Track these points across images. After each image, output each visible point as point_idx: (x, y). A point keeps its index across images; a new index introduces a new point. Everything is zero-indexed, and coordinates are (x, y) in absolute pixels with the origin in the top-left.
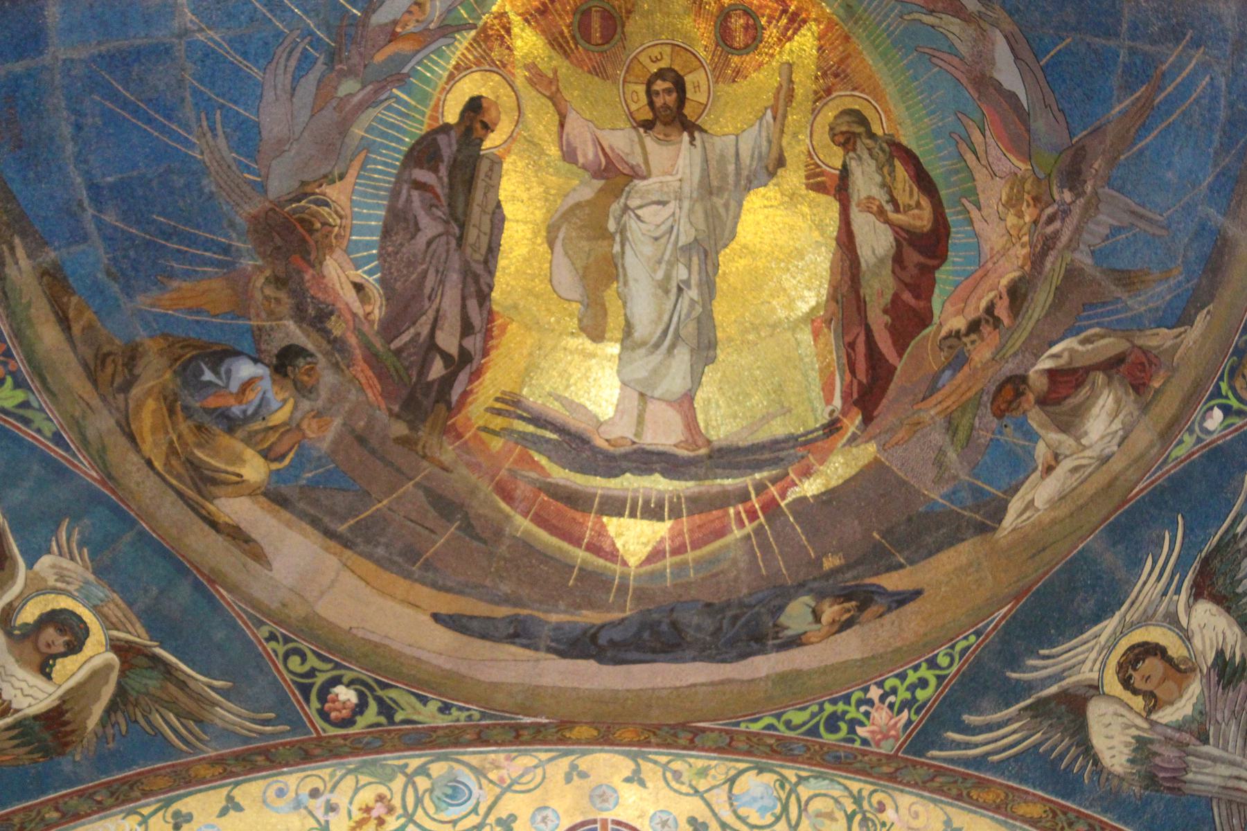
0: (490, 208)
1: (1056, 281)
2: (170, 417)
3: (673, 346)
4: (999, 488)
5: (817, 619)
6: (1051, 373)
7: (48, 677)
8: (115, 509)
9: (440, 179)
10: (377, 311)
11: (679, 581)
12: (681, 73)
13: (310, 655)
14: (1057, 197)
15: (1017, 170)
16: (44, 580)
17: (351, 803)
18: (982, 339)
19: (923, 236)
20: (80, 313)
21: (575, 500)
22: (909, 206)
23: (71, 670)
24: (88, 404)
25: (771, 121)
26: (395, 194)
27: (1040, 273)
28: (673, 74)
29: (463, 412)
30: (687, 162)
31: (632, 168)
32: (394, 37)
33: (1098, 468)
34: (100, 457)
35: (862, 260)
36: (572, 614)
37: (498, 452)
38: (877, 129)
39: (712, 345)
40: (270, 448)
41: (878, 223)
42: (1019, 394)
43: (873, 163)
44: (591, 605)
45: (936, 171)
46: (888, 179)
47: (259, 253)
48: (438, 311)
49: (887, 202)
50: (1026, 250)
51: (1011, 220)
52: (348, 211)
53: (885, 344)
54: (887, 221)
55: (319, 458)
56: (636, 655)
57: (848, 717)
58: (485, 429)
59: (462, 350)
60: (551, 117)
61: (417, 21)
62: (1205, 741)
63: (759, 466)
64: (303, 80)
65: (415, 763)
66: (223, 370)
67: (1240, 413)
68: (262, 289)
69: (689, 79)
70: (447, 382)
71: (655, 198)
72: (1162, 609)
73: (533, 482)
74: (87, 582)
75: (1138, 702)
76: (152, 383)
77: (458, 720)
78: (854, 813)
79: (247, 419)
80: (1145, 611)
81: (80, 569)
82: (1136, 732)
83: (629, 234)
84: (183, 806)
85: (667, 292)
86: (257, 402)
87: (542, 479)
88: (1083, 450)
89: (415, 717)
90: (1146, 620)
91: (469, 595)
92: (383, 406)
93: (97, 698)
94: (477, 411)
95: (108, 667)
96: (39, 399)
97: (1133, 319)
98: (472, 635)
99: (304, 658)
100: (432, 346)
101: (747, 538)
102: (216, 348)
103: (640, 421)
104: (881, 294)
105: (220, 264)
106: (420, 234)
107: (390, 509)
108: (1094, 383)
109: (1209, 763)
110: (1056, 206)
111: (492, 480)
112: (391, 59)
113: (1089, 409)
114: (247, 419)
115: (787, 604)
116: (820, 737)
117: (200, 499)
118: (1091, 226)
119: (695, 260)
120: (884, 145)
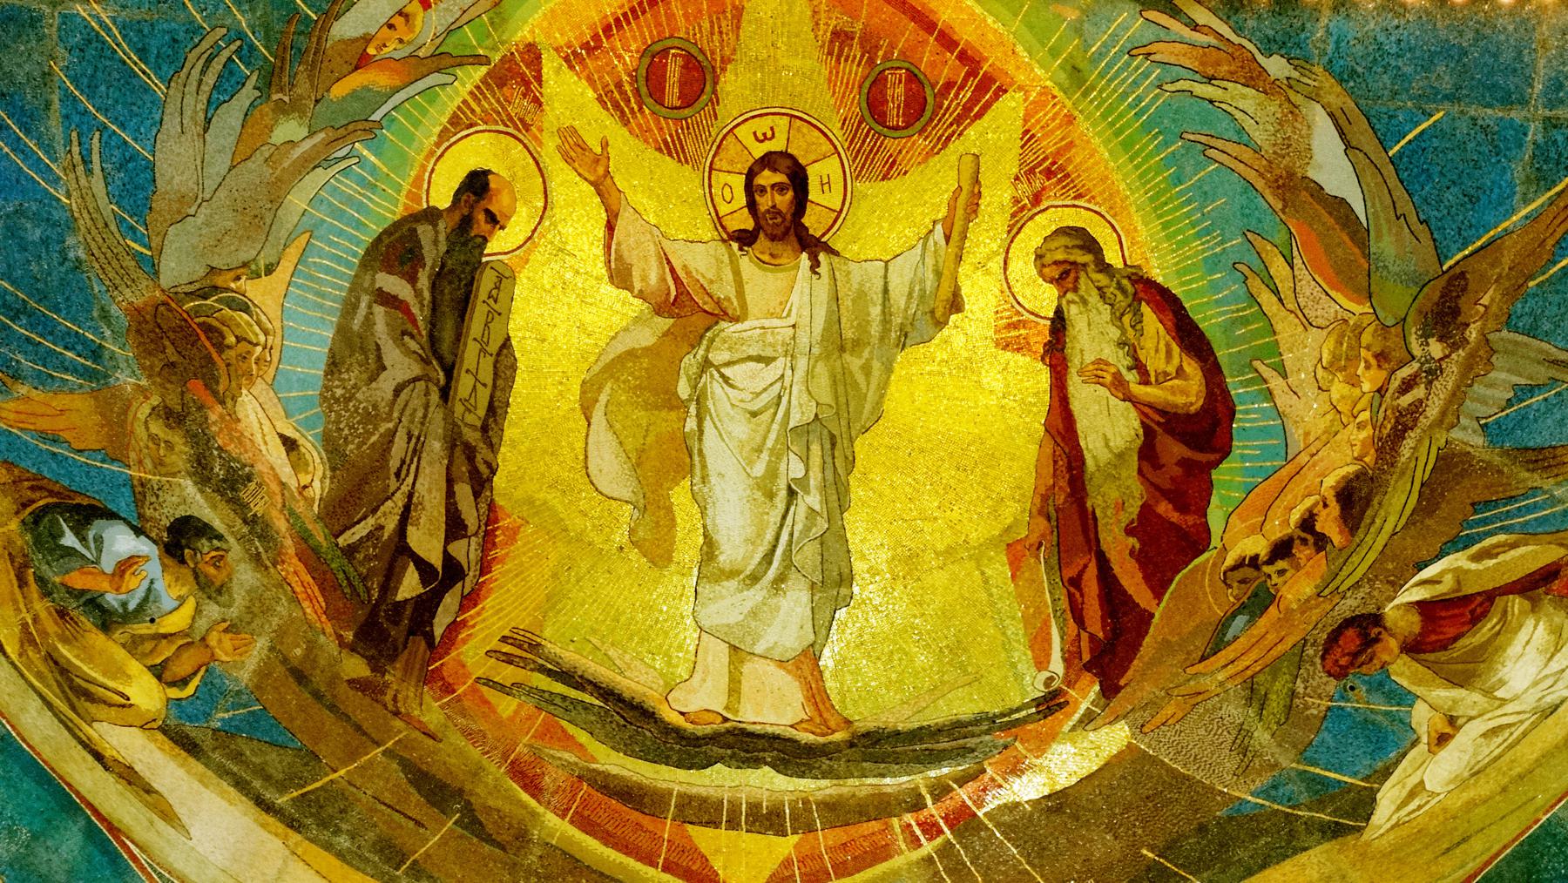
0: (493, 347)
3: (781, 579)
4: (1355, 775)
6: (1421, 605)
9: (418, 294)
10: (317, 484)
12: (803, 162)
14: (1417, 351)
15: (1347, 315)
18: (1298, 568)
22: (1166, 374)
25: (943, 242)
26: (350, 308)
28: (788, 162)
29: (454, 654)
30: (806, 298)
31: (718, 303)
32: (362, 62)
33: (1534, 726)
35: (1087, 456)
37: (512, 719)
38: (1112, 257)
39: (846, 579)
41: (1114, 401)
42: (1369, 642)
45: (1209, 320)
46: (1131, 332)
47: (143, 368)
48: (410, 495)
49: (1130, 369)
50: (1367, 433)
51: (1339, 389)
52: (277, 325)
54: (1128, 398)
55: (239, 693)
58: (488, 682)
59: (448, 558)
61: (401, 41)
63: (935, 758)
66: (91, 535)
69: (813, 173)
70: (426, 606)
71: (753, 352)
73: (567, 765)
79: (128, 617)
83: (710, 404)
85: (771, 496)
87: (582, 764)
88: (1500, 706)
92: (329, 630)
100: (401, 550)
102: (78, 500)
103: (734, 689)
104: (1121, 506)
105: (89, 374)
106: (384, 375)
108: (1505, 612)
110: (1416, 365)
111: (505, 756)
112: (354, 94)
113: (1501, 649)
114: (128, 617)
118: (1478, 388)
119: (815, 448)
120: (1125, 282)
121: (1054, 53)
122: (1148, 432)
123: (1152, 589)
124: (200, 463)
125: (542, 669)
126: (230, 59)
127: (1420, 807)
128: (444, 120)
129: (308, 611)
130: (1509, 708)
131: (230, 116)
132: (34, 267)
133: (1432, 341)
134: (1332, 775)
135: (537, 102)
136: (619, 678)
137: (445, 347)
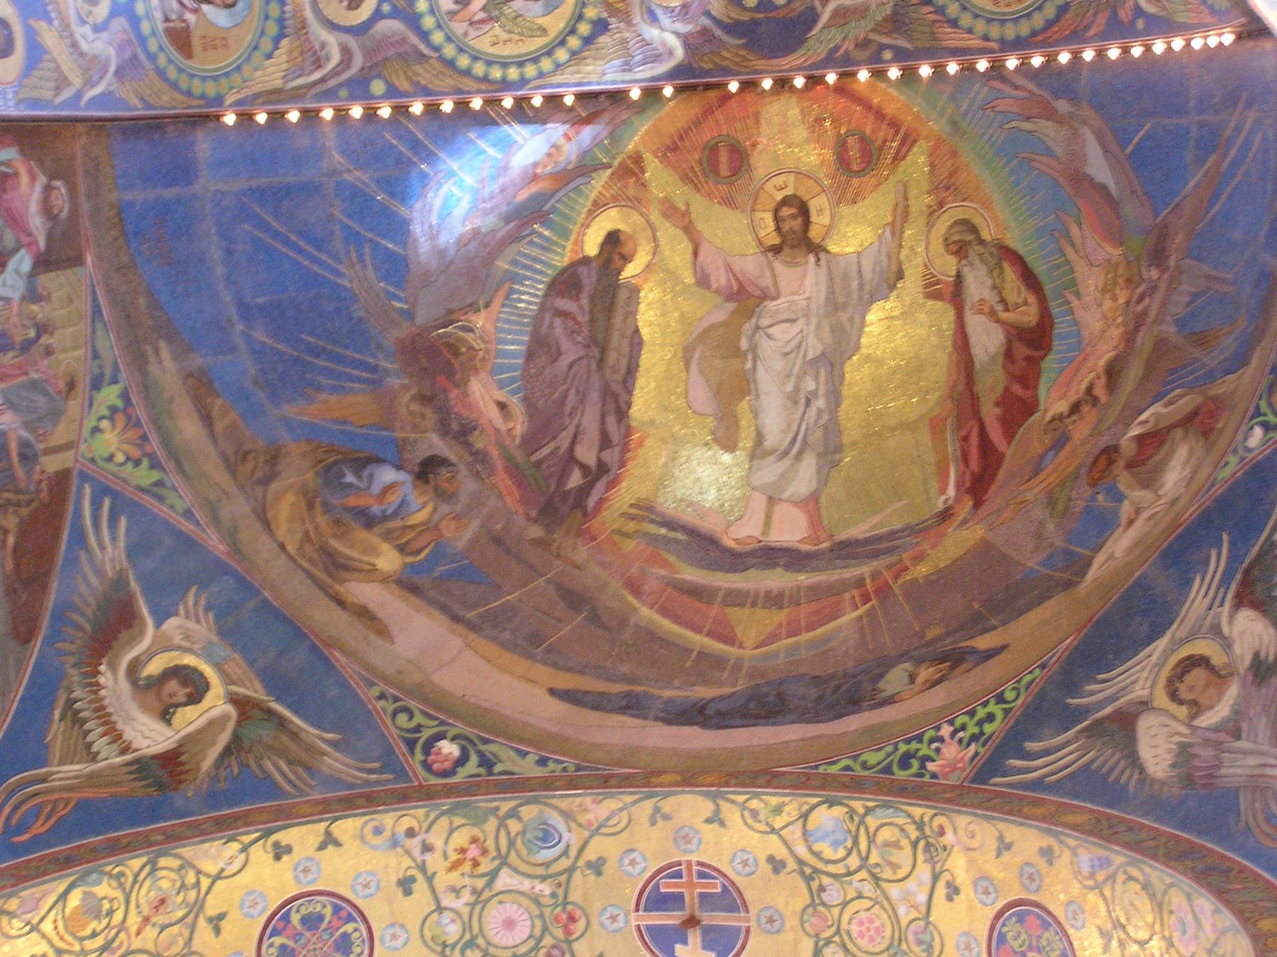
0: (629, 333)
1: (1145, 354)
6: (1140, 439)
7: (168, 722)
8: (241, 580)
9: (581, 307)
10: (518, 427)
13: (417, 713)
14: (1145, 277)
17: (446, 843)
19: (1032, 331)
23: (189, 718)
31: (762, 290)
38: (986, 235)
42: (1111, 462)
44: (705, 682)
45: (1039, 269)
48: (578, 426)
50: (1121, 330)
51: (1108, 304)
53: (996, 435)
54: (998, 321)
55: (455, 555)
56: (739, 721)
57: (921, 753)
58: (620, 532)
60: (685, 246)
62: (1238, 738)
63: (876, 555)
65: (505, 807)
66: (365, 473)
68: (407, 406)
69: (813, 205)
70: (585, 490)
71: (784, 317)
72: (1207, 623)
74: (210, 643)
75: (1182, 711)
76: (292, 480)
77: (553, 772)
78: (918, 840)
79: (385, 518)
82: (1177, 739)
83: (760, 352)
84: (284, 837)
85: (796, 403)
89: (515, 769)
90: (1191, 637)
93: (214, 743)
95: (225, 718)
96: (174, 478)
99: (411, 717)
100: (571, 459)
104: (993, 389)
105: (366, 381)
109: (1239, 756)
114: (385, 518)
116: (892, 774)
117: (329, 581)
119: (822, 373)
120: (993, 250)
121: (942, 114)
122: (1009, 341)
133: (1152, 268)
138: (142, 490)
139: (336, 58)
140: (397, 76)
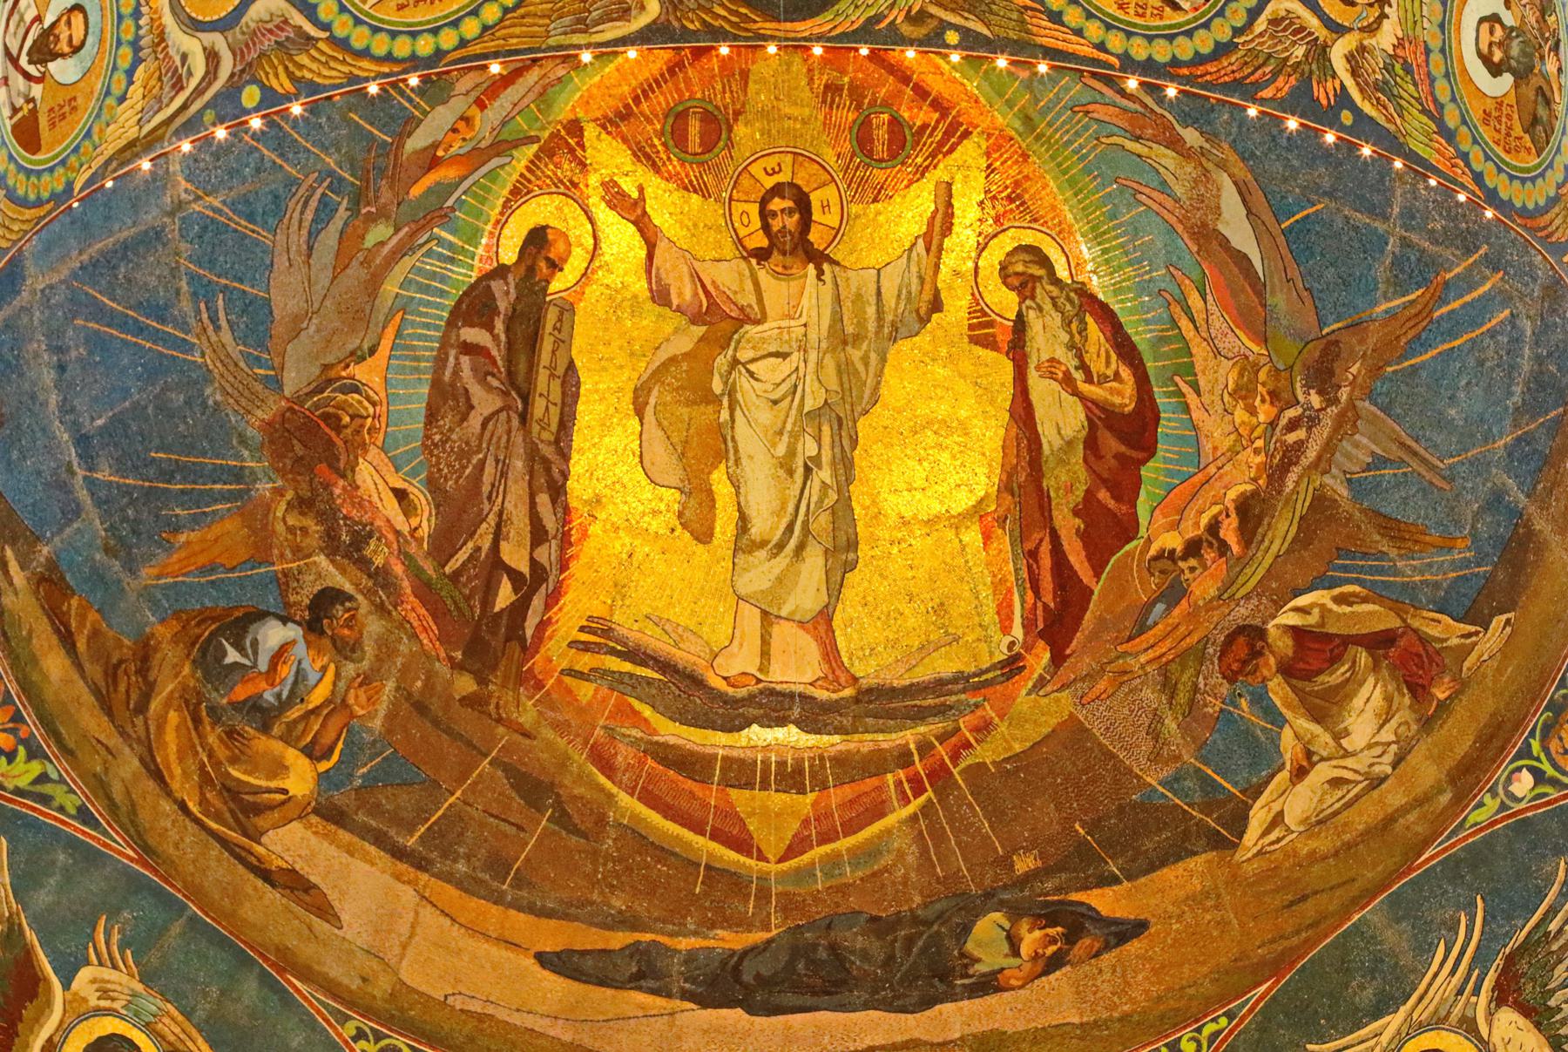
0: (560, 371)
1: (1302, 507)
2: (196, 729)
3: (801, 547)
4: (1235, 784)
5: (1015, 952)
8: (158, 893)
9: (495, 338)
10: (425, 524)
11: (834, 882)
12: (806, 189)
14: (1301, 398)
15: (1248, 353)
16: (85, 1000)
20: (82, 618)
21: (690, 764)
24: (107, 748)
25: (924, 252)
26: (440, 361)
27: (1279, 493)
29: (542, 650)
30: (814, 301)
31: (742, 309)
32: (434, 163)
34: (132, 822)
35: (1044, 441)
36: (706, 937)
37: (590, 704)
39: (853, 545)
40: (314, 741)
41: (1064, 395)
43: (1058, 317)
45: (1141, 336)
47: (277, 470)
49: (1077, 368)
50: (1260, 459)
51: (1240, 415)
52: (383, 394)
53: (1077, 558)
54: (1076, 393)
56: (790, 999)
58: (570, 672)
59: (534, 563)
61: (464, 139)
63: (920, 715)
64: (323, 234)
67: (1554, 782)
68: (284, 519)
69: (815, 198)
71: (772, 349)
72: (1457, 1012)
73: (635, 742)
74: (135, 995)
76: (170, 687)
79: (284, 705)
80: (1436, 1011)
81: (125, 978)
83: (739, 396)
85: (791, 473)
86: (291, 680)
88: (1343, 757)
91: (576, 919)
92: (443, 655)
94: (556, 651)
97: (1405, 586)
98: (585, 982)
100: (497, 564)
101: (913, 818)
102: (238, 614)
103: (765, 654)
104: (1070, 489)
106: (473, 413)
107: (466, 803)
108: (1354, 662)
110: (1300, 410)
111: (586, 742)
112: (429, 191)
113: (1350, 697)
114: (284, 705)
115: (974, 923)
117: (244, 841)
119: (826, 429)
123: (1093, 569)
124: (329, 536)
125: (613, 652)
126: (324, 194)
127: (1278, 840)
128: (505, 192)
129: (425, 641)
130: (1349, 762)
131: (329, 238)
132: (182, 428)
133: (1312, 392)
134: (1218, 779)
135: (583, 165)
136: (674, 650)
137: (521, 378)
138: (19, 792)
139: (199, 66)
140: (277, 76)
